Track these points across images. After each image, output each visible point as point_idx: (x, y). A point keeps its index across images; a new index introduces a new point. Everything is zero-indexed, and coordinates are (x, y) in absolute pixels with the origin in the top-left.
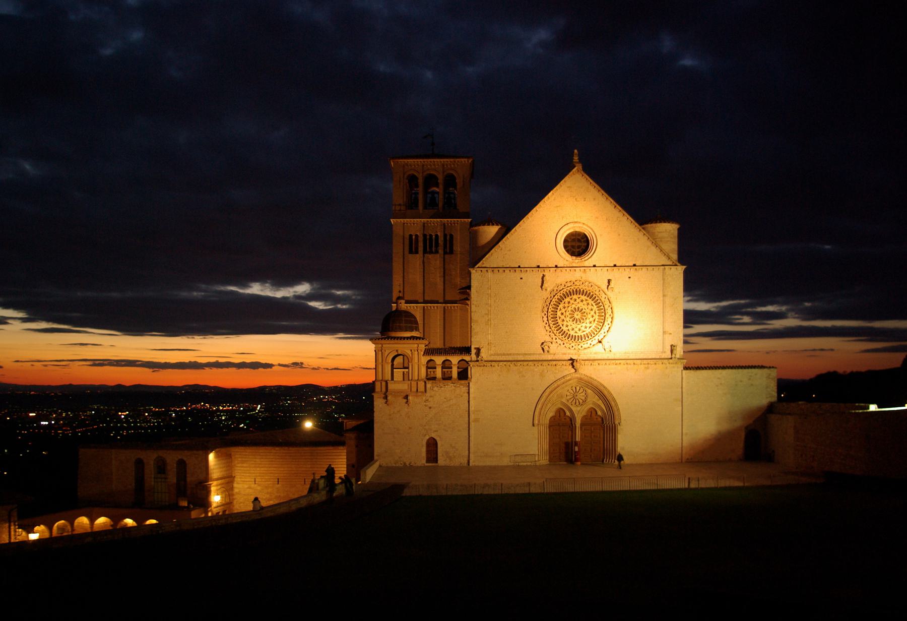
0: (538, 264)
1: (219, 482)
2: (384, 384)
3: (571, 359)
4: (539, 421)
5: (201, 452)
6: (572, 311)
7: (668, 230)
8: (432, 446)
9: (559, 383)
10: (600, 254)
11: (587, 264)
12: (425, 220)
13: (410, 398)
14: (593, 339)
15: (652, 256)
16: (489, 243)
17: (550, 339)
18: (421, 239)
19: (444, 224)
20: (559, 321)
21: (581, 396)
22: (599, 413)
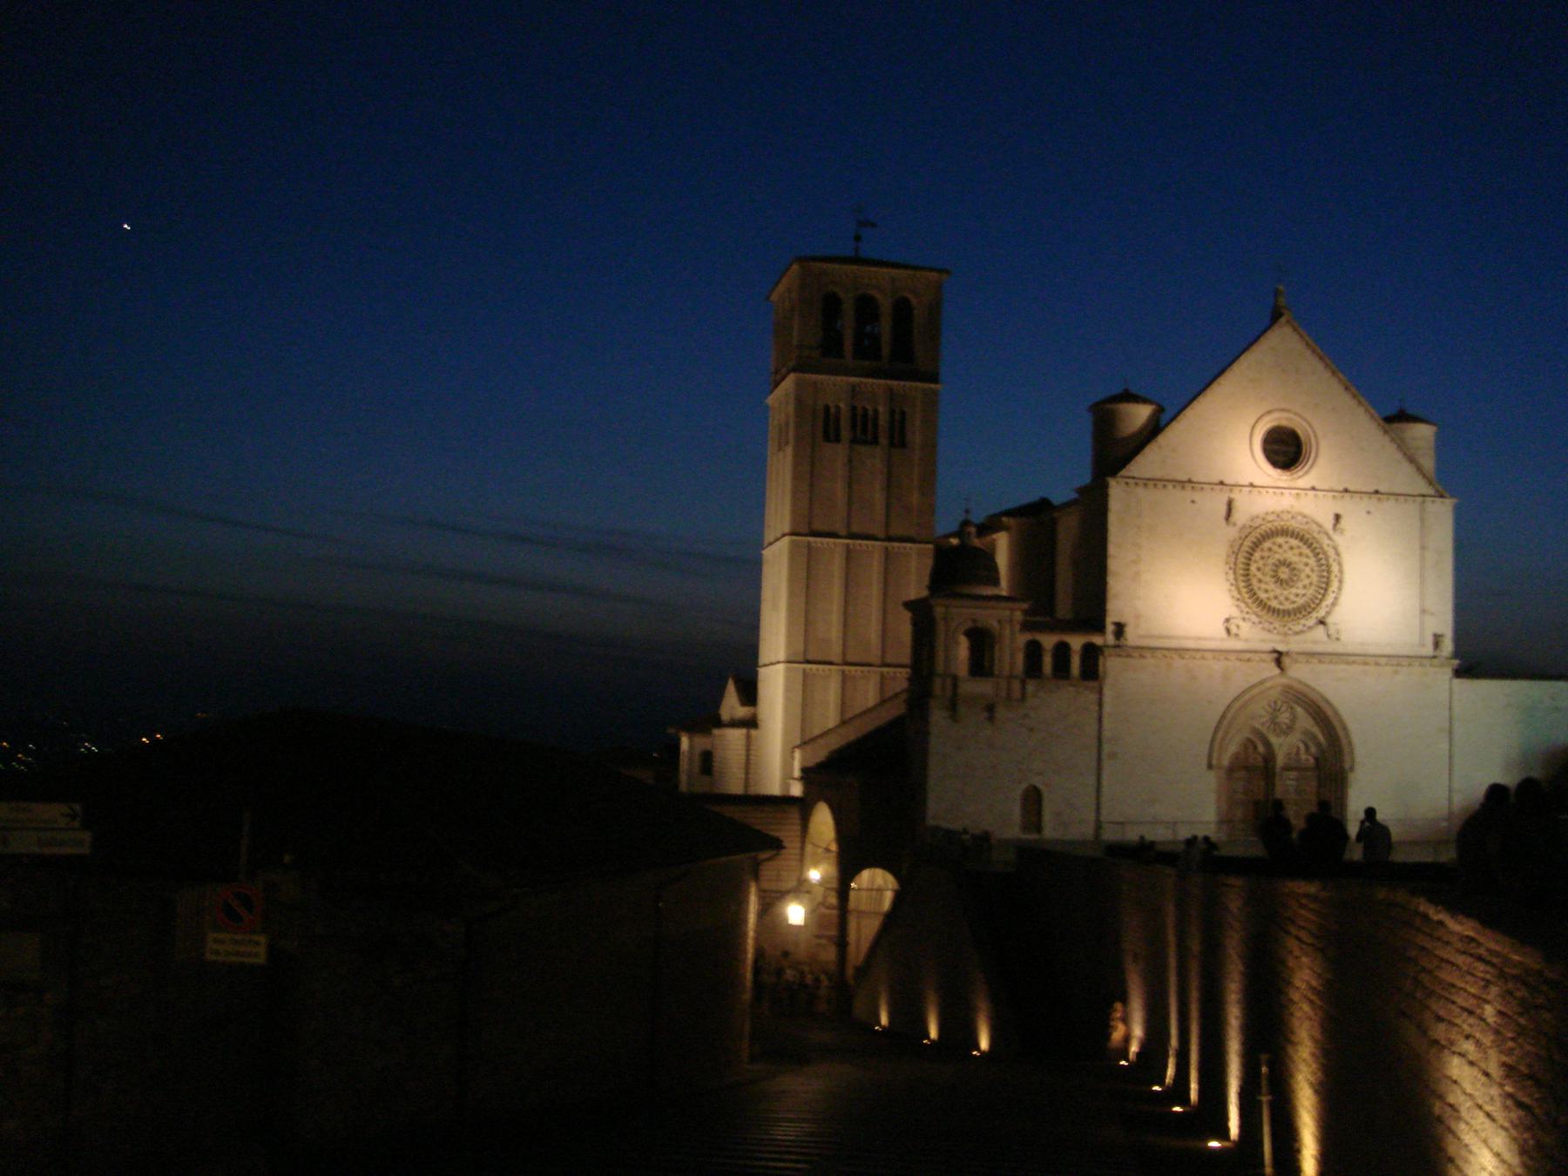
2: (949, 682)
3: (1275, 651)
8: (1033, 800)
15: (1406, 479)
16: (1140, 432)
21: (1284, 717)
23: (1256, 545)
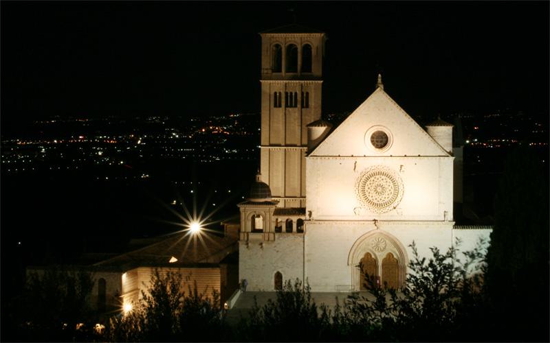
1: (130, 294)
2: (246, 234)
3: (375, 220)
4: (352, 261)
5: (116, 274)
7: (444, 132)
8: (279, 276)
9: (366, 236)
10: (394, 148)
12: (287, 81)
13: (264, 245)
15: (433, 149)
16: (319, 138)
18: (283, 96)
19: (302, 84)
21: (382, 245)
22: (395, 257)
23: (367, 179)
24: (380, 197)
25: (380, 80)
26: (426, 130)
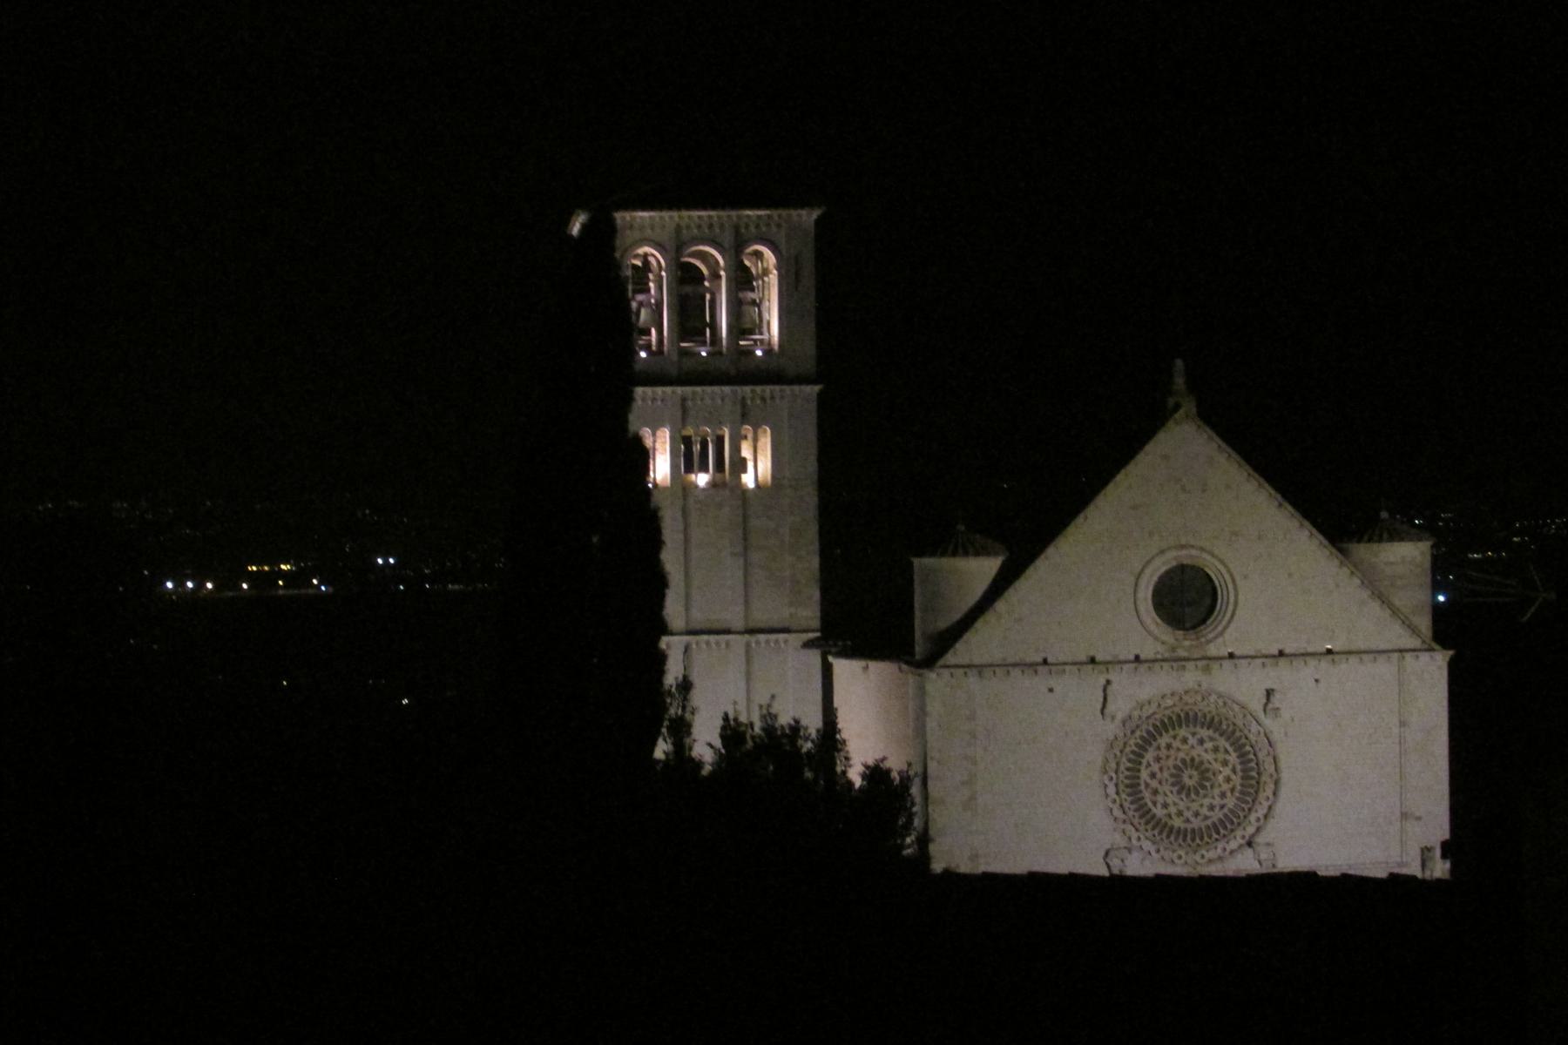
0: (1092, 654)
6: (1176, 767)
11: (1213, 650)
14: (1232, 836)
17: (1123, 843)
19: (743, 398)
20: (1147, 795)
23: (1148, 740)
24: (1195, 806)
25: (1179, 382)
26: (1341, 551)
